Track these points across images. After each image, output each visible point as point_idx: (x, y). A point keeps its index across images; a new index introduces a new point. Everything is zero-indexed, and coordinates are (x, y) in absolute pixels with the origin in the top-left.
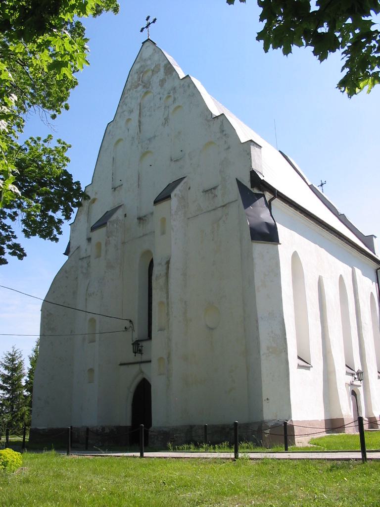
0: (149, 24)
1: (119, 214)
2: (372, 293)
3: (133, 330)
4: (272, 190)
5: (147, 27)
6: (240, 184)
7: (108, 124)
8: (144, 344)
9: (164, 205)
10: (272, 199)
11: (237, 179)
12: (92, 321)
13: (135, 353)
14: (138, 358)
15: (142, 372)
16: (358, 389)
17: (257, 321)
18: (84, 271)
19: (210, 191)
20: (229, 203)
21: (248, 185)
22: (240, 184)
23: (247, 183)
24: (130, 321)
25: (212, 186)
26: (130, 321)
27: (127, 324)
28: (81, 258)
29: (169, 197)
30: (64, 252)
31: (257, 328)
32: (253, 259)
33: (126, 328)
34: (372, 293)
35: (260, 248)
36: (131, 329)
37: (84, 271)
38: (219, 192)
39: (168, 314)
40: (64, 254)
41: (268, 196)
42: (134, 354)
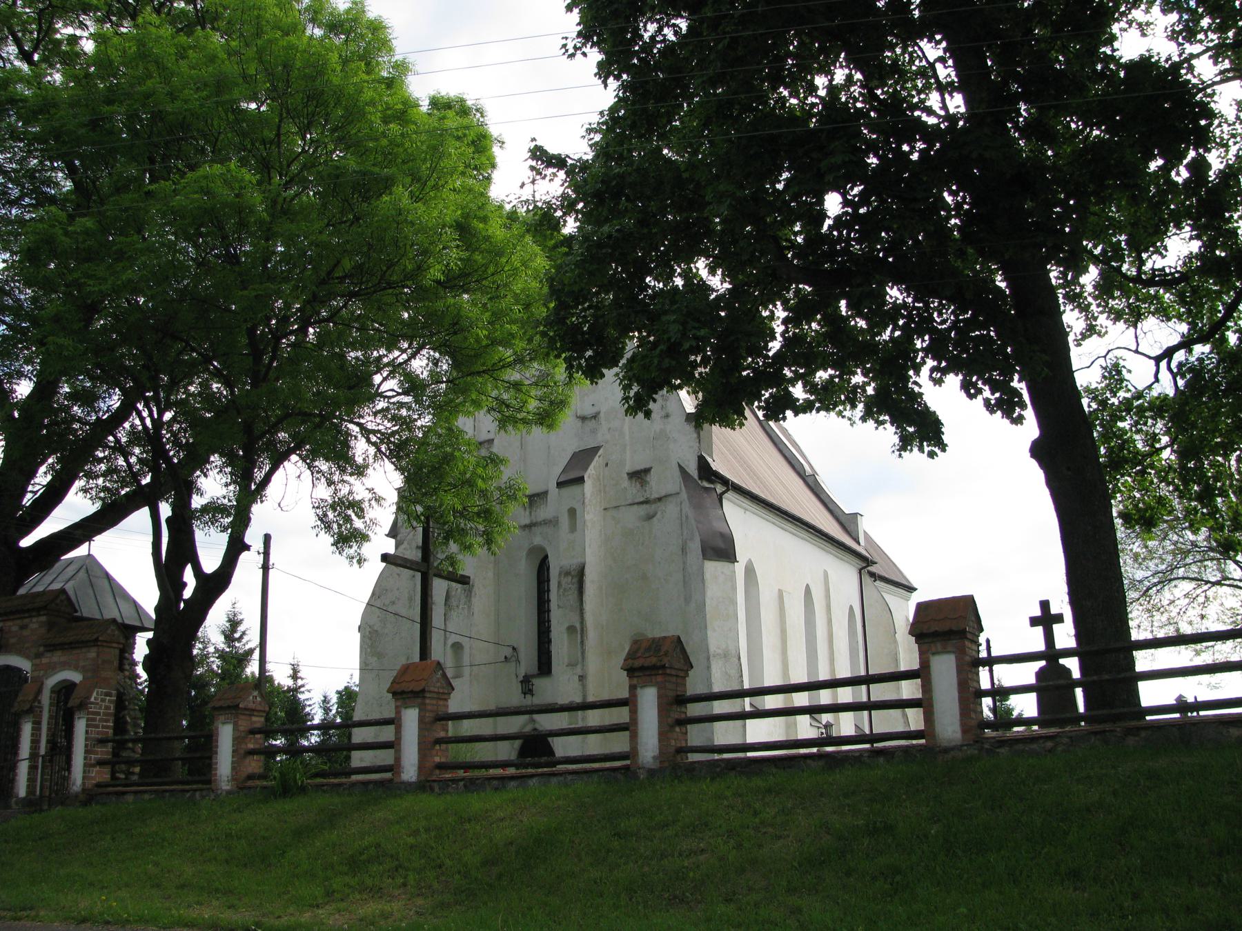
2: (851, 608)
3: (518, 661)
4: (725, 481)
6: (683, 471)
8: (535, 681)
9: (573, 490)
10: (724, 493)
13: (525, 694)
14: (528, 701)
15: (533, 721)
17: (708, 659)
19: (640, 475)
20: (665, 496)
22: (683, 471)
23: (694, 472)
24: (514, 649)
25: (642, 467)
26: (514, 649)
27: (508, 652)
29: (580, 480)
31: (709, 667)
32: (703, 580)
33: (506, 657)
34: (851, 608)
35: (713, 568)
36: (514, 659)
38: (653, 478)
39: (582, 642)
40: (387, 535)
41: (720, 488)
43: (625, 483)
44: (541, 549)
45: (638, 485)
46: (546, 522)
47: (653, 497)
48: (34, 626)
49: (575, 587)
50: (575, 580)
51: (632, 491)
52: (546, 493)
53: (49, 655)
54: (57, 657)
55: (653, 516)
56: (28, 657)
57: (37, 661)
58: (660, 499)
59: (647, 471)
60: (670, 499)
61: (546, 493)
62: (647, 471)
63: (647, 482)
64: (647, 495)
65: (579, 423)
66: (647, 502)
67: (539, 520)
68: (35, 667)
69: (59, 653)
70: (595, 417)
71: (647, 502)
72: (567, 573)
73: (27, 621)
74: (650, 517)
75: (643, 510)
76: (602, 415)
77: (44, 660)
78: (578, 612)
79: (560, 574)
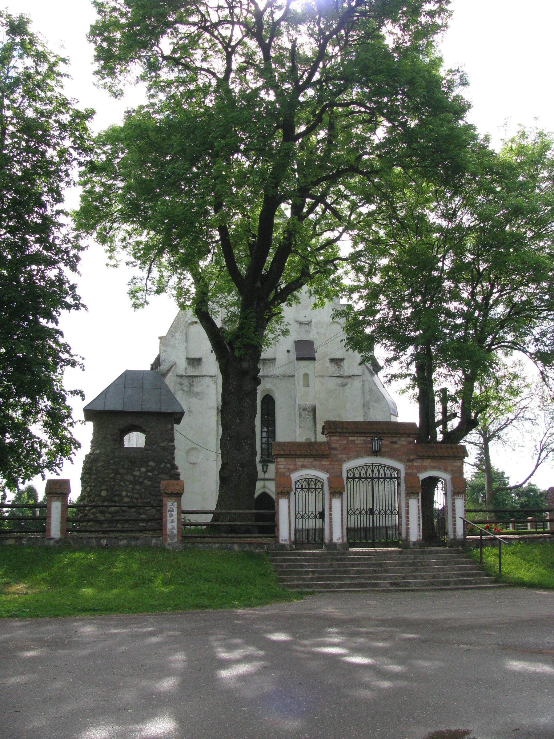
15: (264, 487)
18: (186, 389)
28: (180, 374)
37: (186, 389)
38: (345, 364)
43: (328, 364)
44: (270, 390)
45: (336, 367)
46: (273, 376)
47: (345, 375)
48: (404, 443)
49: (311, 417)
50: (311, 414)
51: (332, 369)
52: (275, 359)
53: (419, 461)
54: (427, 463)
55: (346, 385)
56: (400, 460)
57: (410, 464)
58: (350, 377)
59: (342, 360)
60: (356, 378)
61: (275, 359)
62: (342, 360)
63: (341, 366)
64: (342, 373)
65: (297, 325)
66: (341, 377)
67: (269, 374)
68: (407, 468)
69: (429, 461)
70: (309, 323)
71: (341, 377)
72: (305, 409)
73: (395, 439)
74: (344, 385)
75: (339, 381)
76: (313, 323)
77: (415, 464)
78: (313, 431)
79: (300, 409)
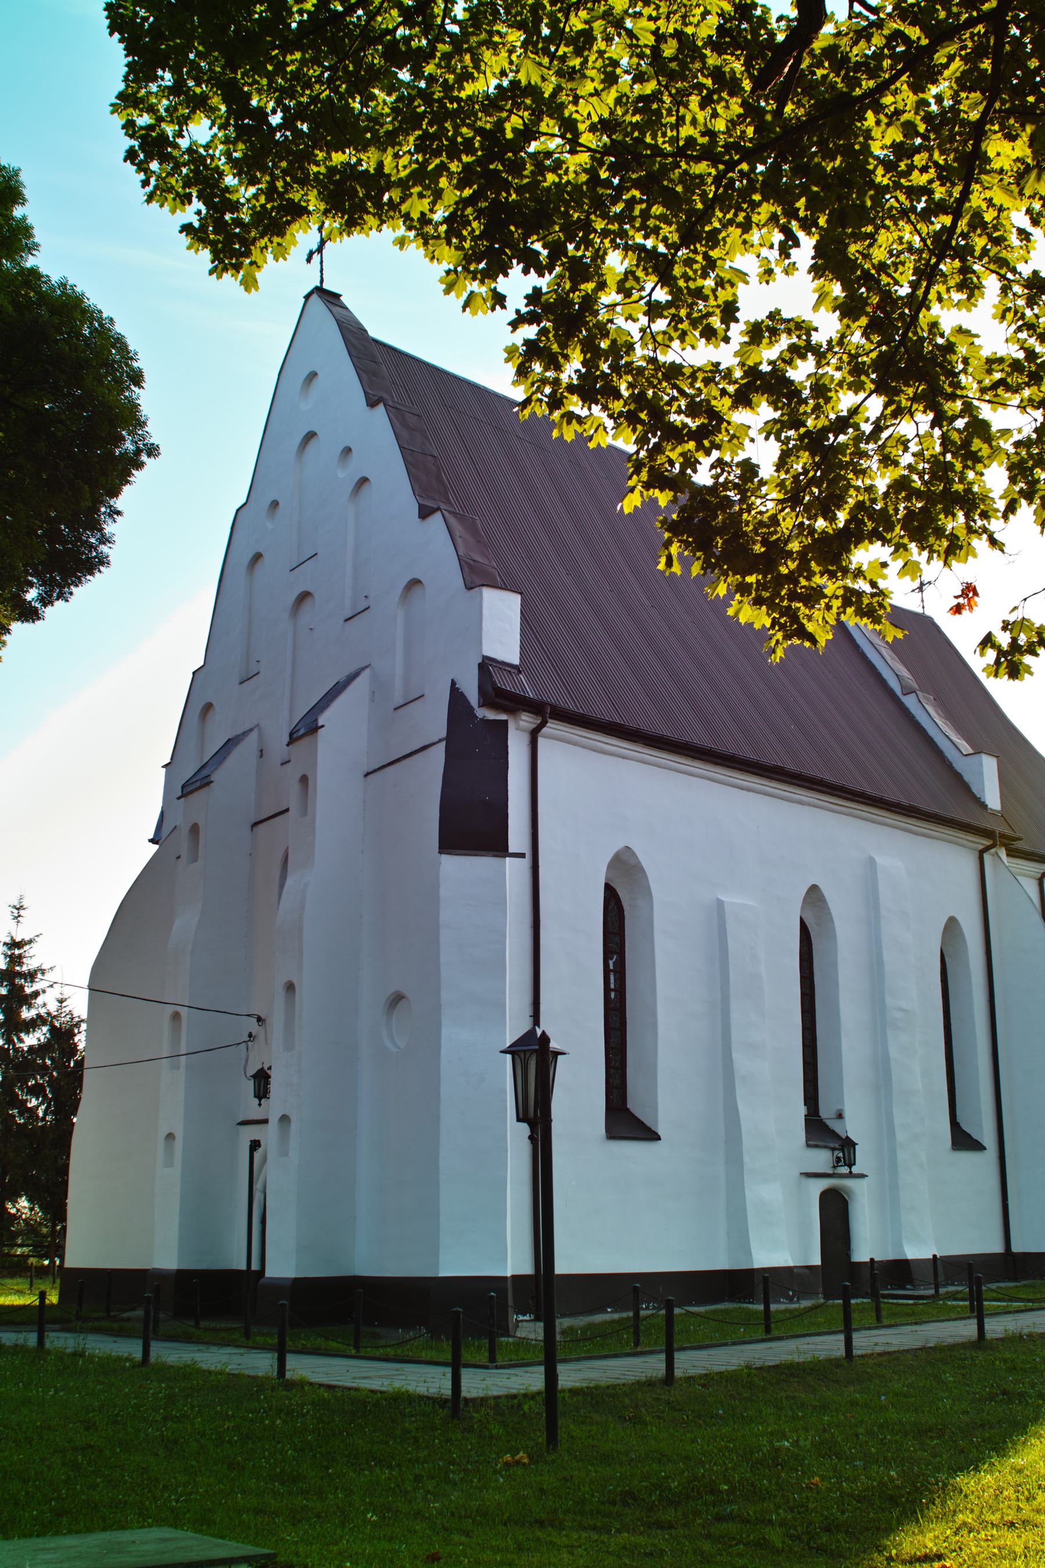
0: (323, 242)
1: (245, 753)
5: (320, 250)
6: (456, 695)
7: (238, 511)
11: (453, 683)
12: (176, 1016)
16: (849, 1191)
21: (472, 695)
22: (456, 695)
23: (472, 695)
24: (259, 1019)
26: (259, 1019)
30: (151, 837)
34: (952, 926)
40: (151, 841)
42: (257, 1101)
